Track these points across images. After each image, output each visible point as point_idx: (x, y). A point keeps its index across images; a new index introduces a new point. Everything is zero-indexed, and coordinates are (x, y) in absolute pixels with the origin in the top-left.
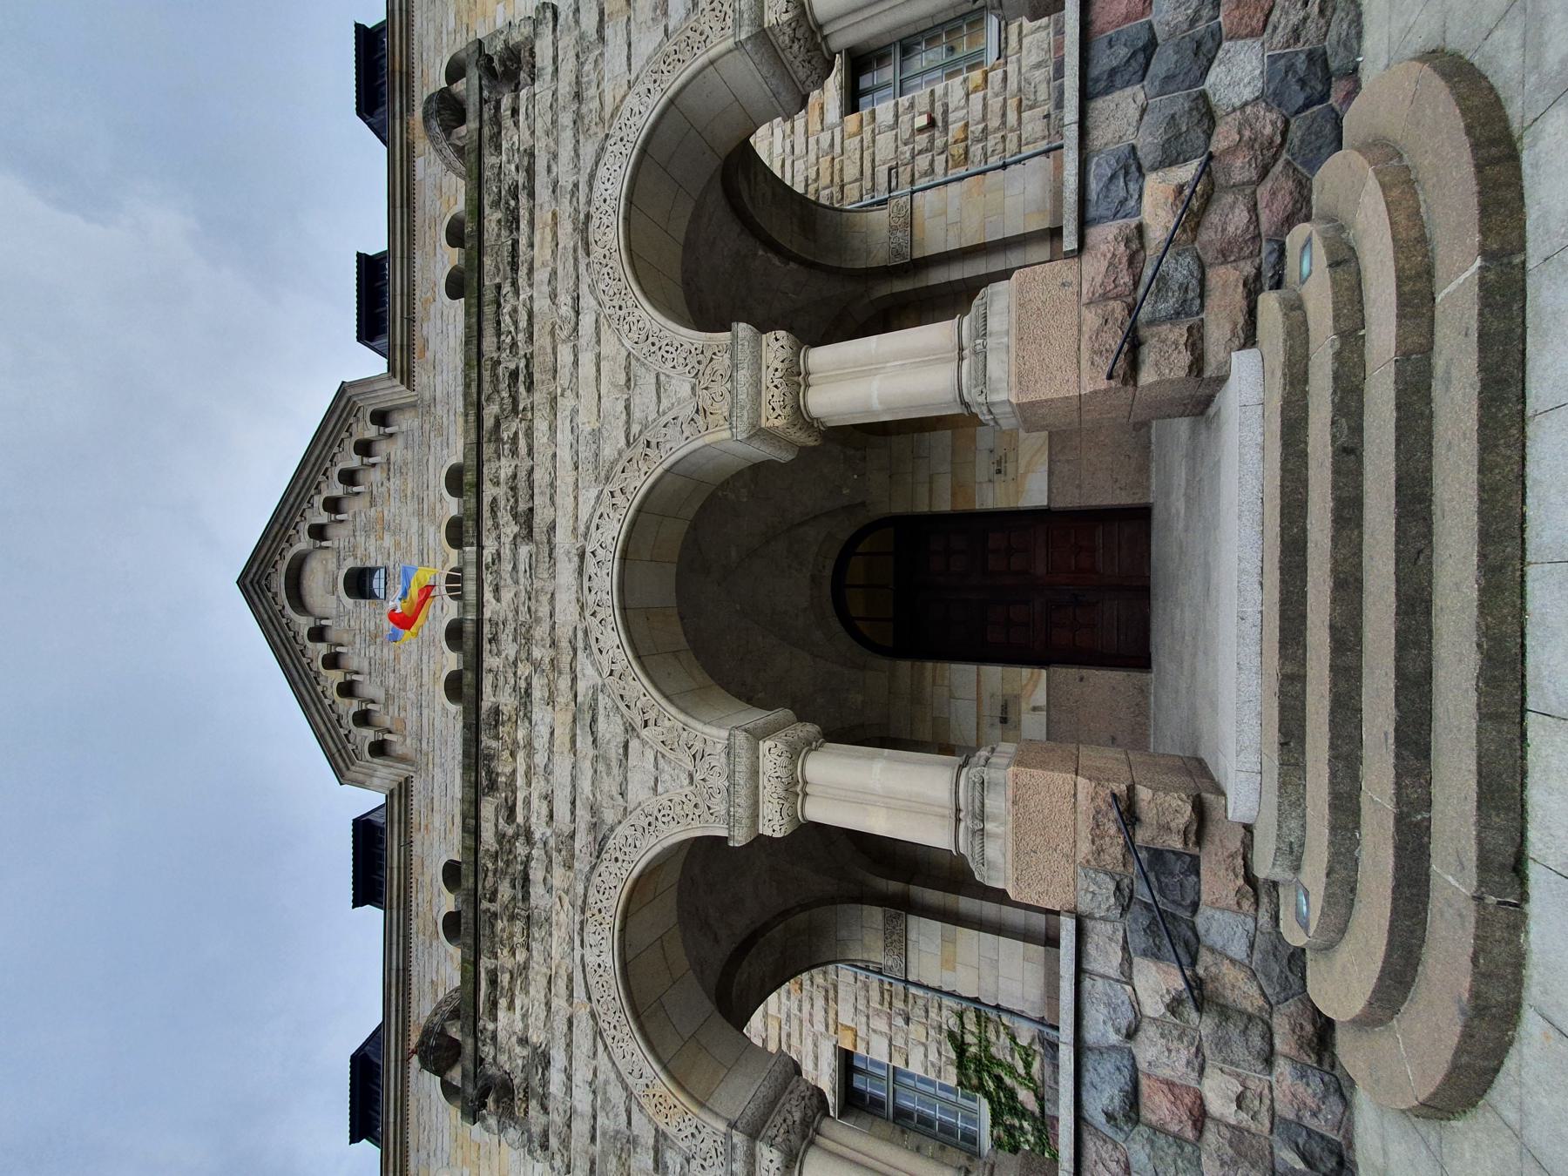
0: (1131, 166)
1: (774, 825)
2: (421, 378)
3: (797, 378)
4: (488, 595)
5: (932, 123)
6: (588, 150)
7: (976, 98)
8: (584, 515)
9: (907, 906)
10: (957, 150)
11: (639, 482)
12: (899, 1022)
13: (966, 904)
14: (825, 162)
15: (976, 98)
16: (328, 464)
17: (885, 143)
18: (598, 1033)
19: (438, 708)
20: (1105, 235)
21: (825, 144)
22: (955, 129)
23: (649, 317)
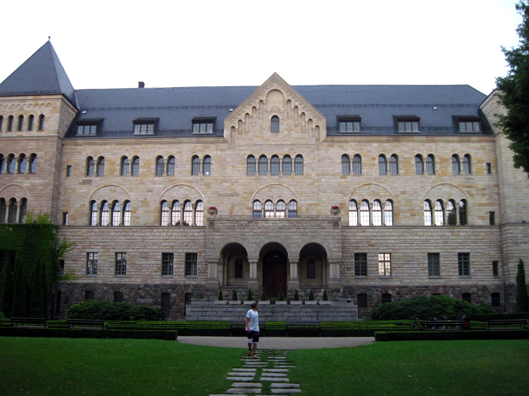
0: (305, 291)
1: (250, 261)
2: (326, 144)
3: (294, 263)
4: (272, 222)
5: (349, 268)
6: (322, 237)
7: (350, 275)
8: (282, 237)
9: (224, 265)
10: (343, 272)
11: (284, 245)
12: (204, 263)
13: (226, 274)
14: (348, 250)
15: (350, 275)
16: (307, 109)
17: (348, 260)
18: (224, 239)
19: (246, 152)
20: (300, 289)
21: (350, 250)
22: (347, 272)
23: (303, 246)
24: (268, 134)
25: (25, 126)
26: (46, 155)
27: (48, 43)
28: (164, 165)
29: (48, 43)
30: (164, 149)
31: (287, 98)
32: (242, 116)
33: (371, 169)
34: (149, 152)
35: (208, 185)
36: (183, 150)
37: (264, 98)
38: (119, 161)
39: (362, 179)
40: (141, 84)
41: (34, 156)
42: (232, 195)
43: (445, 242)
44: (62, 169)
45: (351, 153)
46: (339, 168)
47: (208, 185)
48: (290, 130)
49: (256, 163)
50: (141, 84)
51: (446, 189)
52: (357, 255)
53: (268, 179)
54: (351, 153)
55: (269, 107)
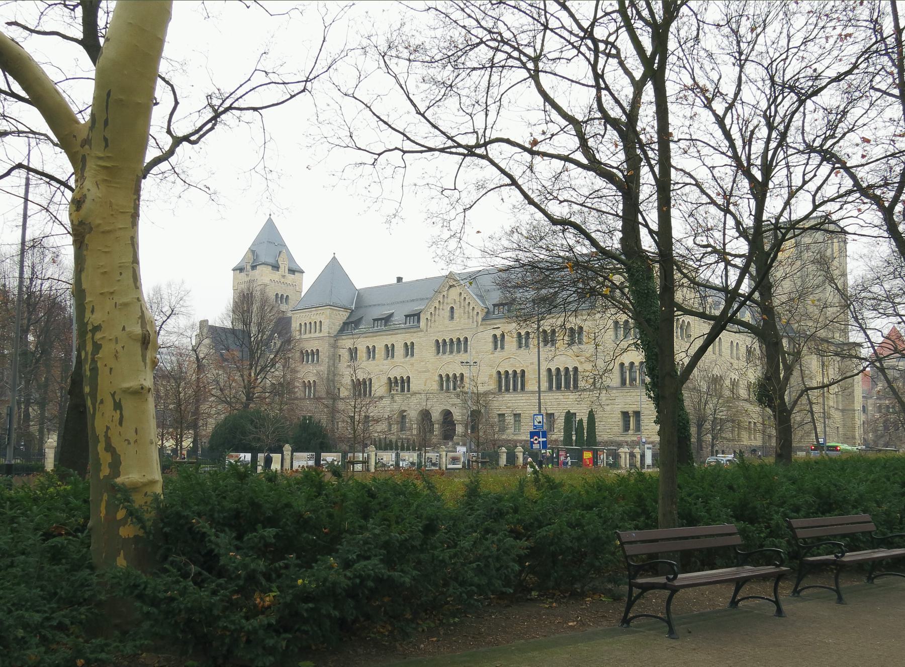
24: (447, 321)
25: (313, 330)
26: (324, 349)
27: (334, 258)
28: (390, 351)
29: (334, 258)
30: (388, 340)
31: (459, 291)
32: (432, 310)
33: (511, 343)
34: (380, 342)
35: (412, 364)
36: (399, 340)
37: (445, 293)
38: (365, 350)
39: (504, 354)
40: (399, 279)
41: (318, 350)
42: (425, 372)
43: (559, 404)
44: (335, 358)
45: (498, 333)
46: (491, 346)
47: (412, 364)
48: (460, 318)
49: (441, 347)
50: (399, 279)
51: (563, 358)
52: (499, 415)
53: (447, 357)
54: (498, 333)
55: (449, 300)
